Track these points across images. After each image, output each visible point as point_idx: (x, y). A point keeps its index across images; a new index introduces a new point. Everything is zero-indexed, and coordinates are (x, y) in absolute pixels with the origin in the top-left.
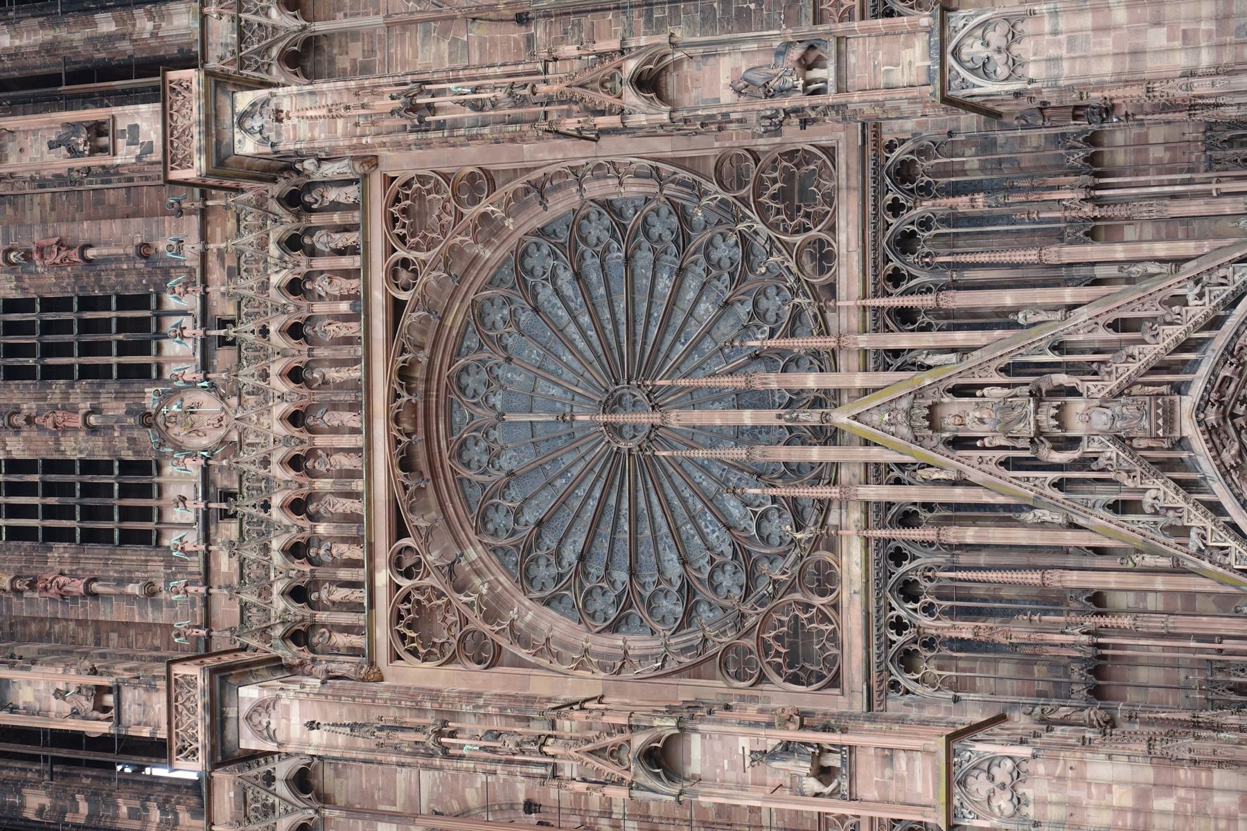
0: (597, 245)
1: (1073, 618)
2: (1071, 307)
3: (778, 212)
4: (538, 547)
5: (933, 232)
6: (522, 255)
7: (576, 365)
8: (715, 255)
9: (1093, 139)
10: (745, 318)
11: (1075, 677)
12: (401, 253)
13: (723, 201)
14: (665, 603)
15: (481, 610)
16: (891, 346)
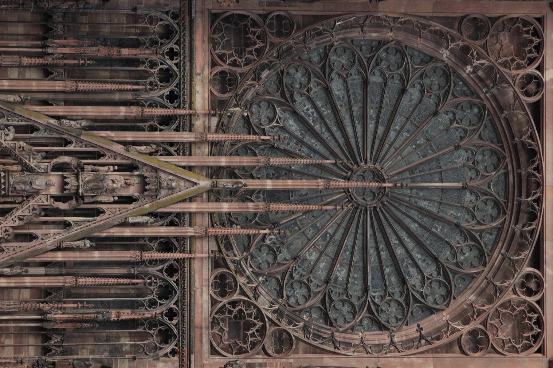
0: (390, 300)
1: (61, 62)
2: (59, 249)
3: (250, 315)
4: (439, 97)
5: (147, 298)
6: (448, 296)
7: (407, 221)
8: (304, 291)
9: (46, 351)
10: (284, 250)
11: (60, 26)
12: (532, 300)
13: (290, 323)
14: (344, 62)
15: (472, 55)
16: (172, 229)
